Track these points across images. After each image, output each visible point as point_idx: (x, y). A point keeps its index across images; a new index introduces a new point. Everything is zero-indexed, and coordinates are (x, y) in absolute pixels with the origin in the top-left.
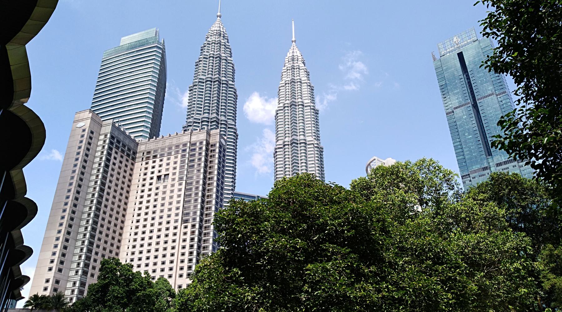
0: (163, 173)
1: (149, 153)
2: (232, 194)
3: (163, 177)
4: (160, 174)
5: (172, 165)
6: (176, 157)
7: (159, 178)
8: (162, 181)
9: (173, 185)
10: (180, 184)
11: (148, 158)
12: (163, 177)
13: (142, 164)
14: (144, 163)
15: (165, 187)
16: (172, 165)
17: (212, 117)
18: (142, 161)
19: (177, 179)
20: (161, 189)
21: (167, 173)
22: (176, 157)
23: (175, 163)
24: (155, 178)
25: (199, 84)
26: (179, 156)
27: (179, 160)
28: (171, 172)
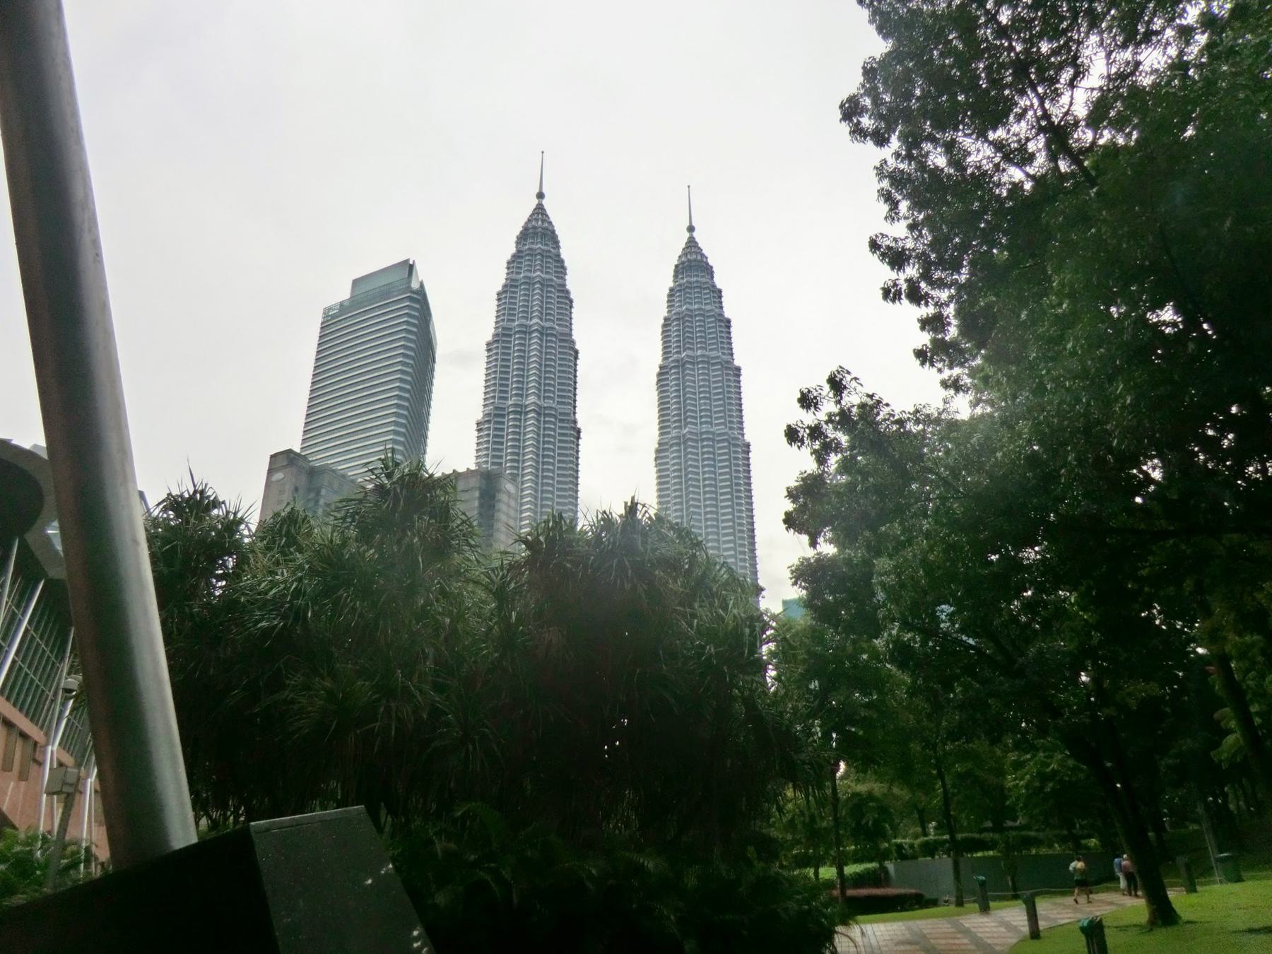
17: (527, 403)
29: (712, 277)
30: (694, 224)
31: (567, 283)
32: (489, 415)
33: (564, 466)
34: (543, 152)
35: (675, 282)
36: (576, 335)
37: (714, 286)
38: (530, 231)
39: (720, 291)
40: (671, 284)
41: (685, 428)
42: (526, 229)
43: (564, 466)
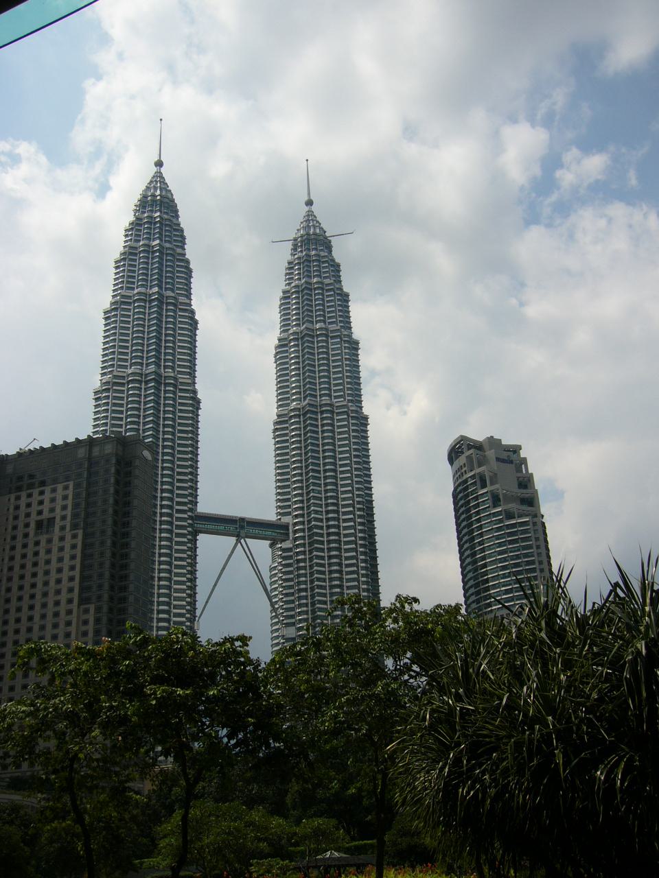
0: (46, 515)
1: (20, 478)
2: (191, 518)
3: (45, 523)
4: (40, 518)
5: (59, 503)
6: (66, 488)
7: (39, 525)
8: (44, 530)
9: (62, 539)
10: (74, 536)
11: (19, 489)
12: (45, 523)
13: (9, 500)
14: (13, 497)
15: (50, 541)
16: (59, 503)
17: (147, 372)
18: (10, 493)
19: (68, 528)
20: (43, 543)
21: (52, 515)
22: (66, 488)
23: (65, 498)
24: (33, 525)
25: (122, 306)
26: (71, 484)
27: (70, 492)
28: (58, 512)
29: (330, 252)
30: (312, 198)
31: (187, 251)
32: (107, 383)
33: (185, 435)
34: (161, 120)
35: (293, 255)
36: (195, 304)
37: (333, 260)
38: (149, 198)
39: (339, 266)
40: (290, 258)
41: (304, 400)
42: (145, 197)
43: (185, 435)
